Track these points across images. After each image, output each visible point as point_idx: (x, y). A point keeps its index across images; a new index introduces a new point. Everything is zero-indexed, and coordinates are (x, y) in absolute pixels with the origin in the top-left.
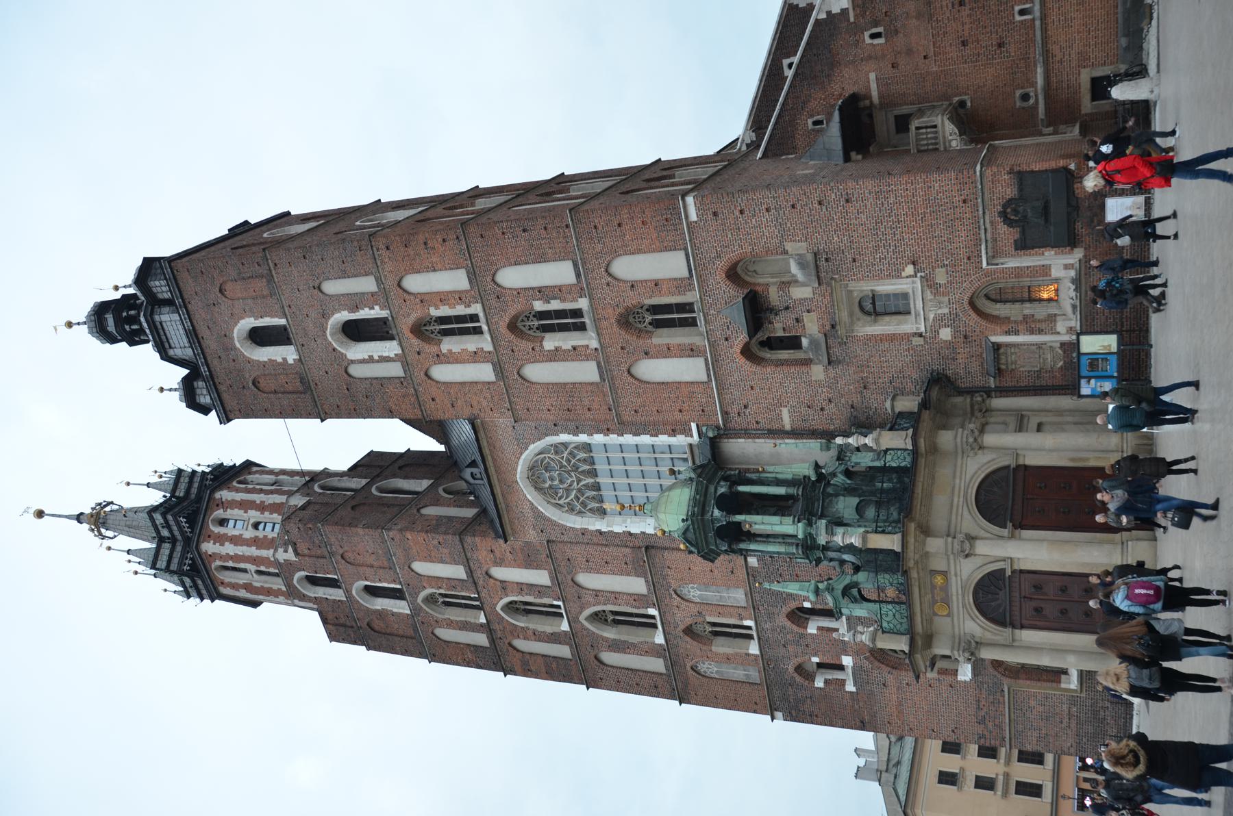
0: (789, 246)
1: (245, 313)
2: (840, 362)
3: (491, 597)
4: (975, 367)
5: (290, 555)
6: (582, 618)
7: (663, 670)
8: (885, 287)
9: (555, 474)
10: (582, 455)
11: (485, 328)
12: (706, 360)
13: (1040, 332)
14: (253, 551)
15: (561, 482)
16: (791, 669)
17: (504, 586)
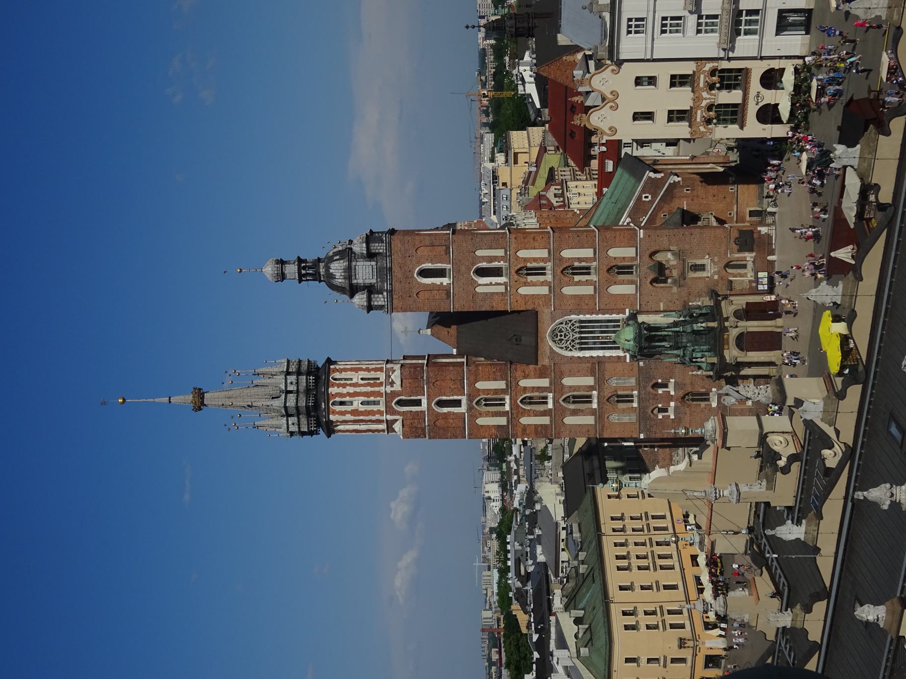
0: (672, 248)
1: (427, 261)
2: (682, 286)
3: (516, 396)
4: (724, 288)
5: (397, 387)
6: (560, 401)
7: (593, 423)
8: (699, 262)
9: (563, 334)
11: (549, 272)
12: (637, 286)
13: (743, 277)
14: (369, 389)
15: (565, 337)
16: (650, 411)
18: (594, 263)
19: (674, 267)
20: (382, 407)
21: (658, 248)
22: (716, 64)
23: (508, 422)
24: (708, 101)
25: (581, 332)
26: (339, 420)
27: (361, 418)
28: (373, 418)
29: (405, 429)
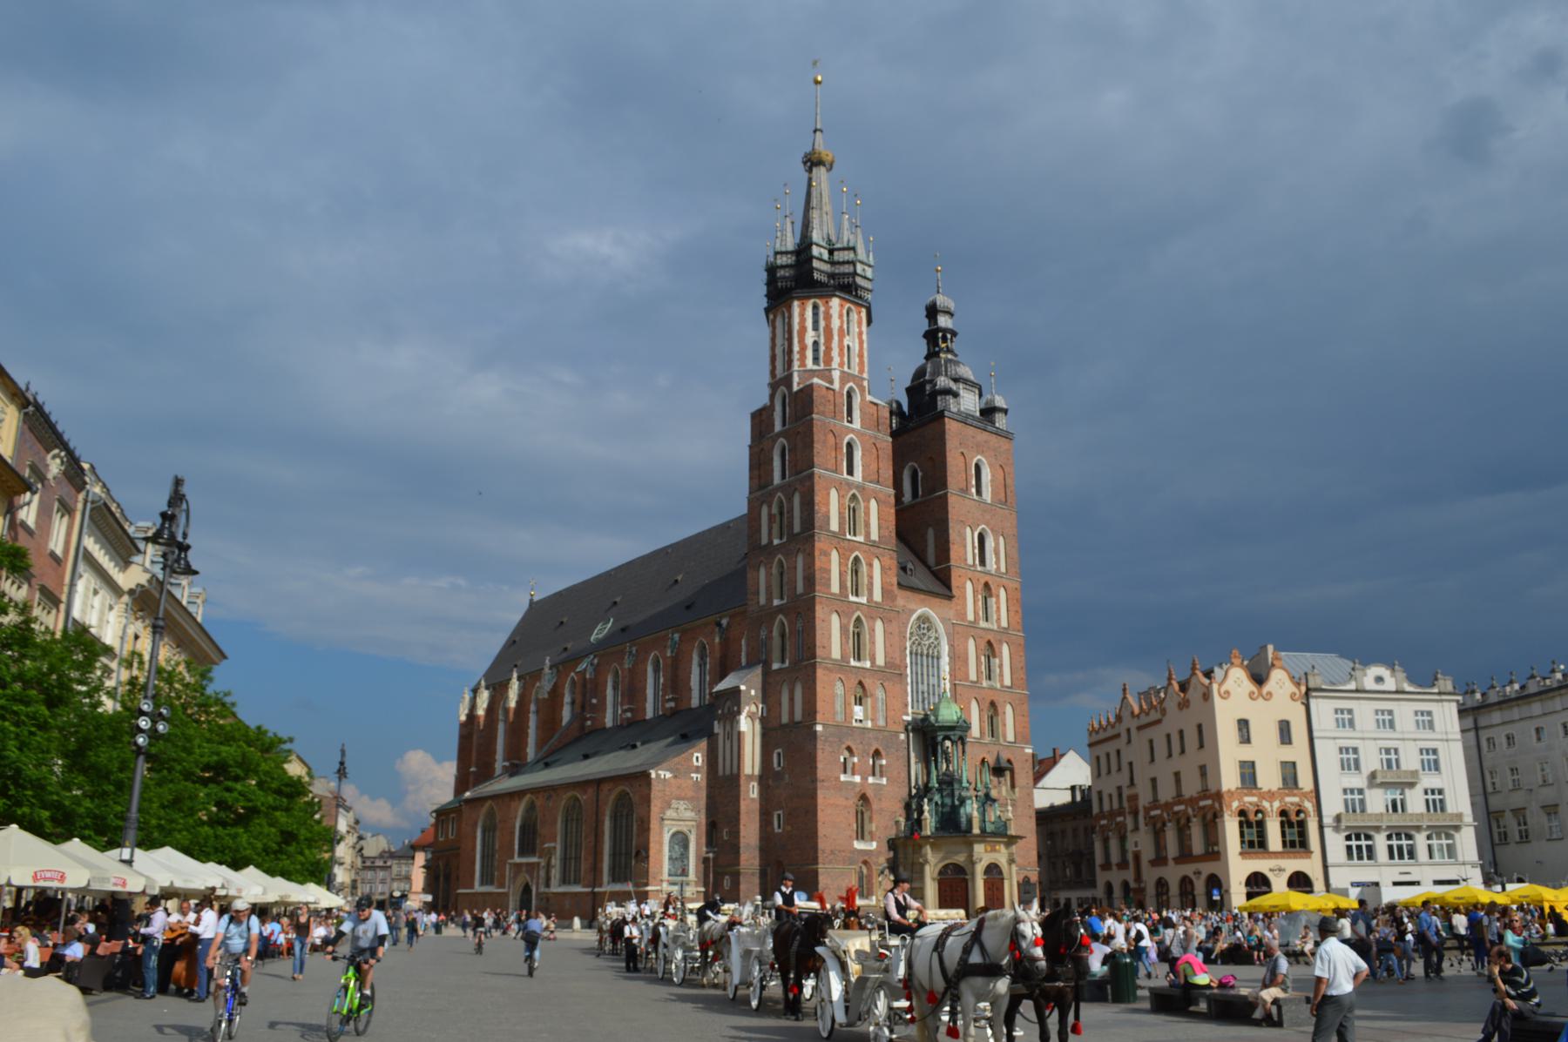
1: (993, 476)
6: (858, 613)
9: (925, 631)
10: (936, 654)
16: (849, 743)
17: (870, 565)
18: (998, 686)
19: (1000, 792)
20: (846, 369)
21: (1016, 771)
22: (1312, 814)
23: (834, 532)
24: (1269, 809)
25: (928, 656)
26: (832, 311)
27: (836, 338)
28: (835, 353)
29: (824, 390)
